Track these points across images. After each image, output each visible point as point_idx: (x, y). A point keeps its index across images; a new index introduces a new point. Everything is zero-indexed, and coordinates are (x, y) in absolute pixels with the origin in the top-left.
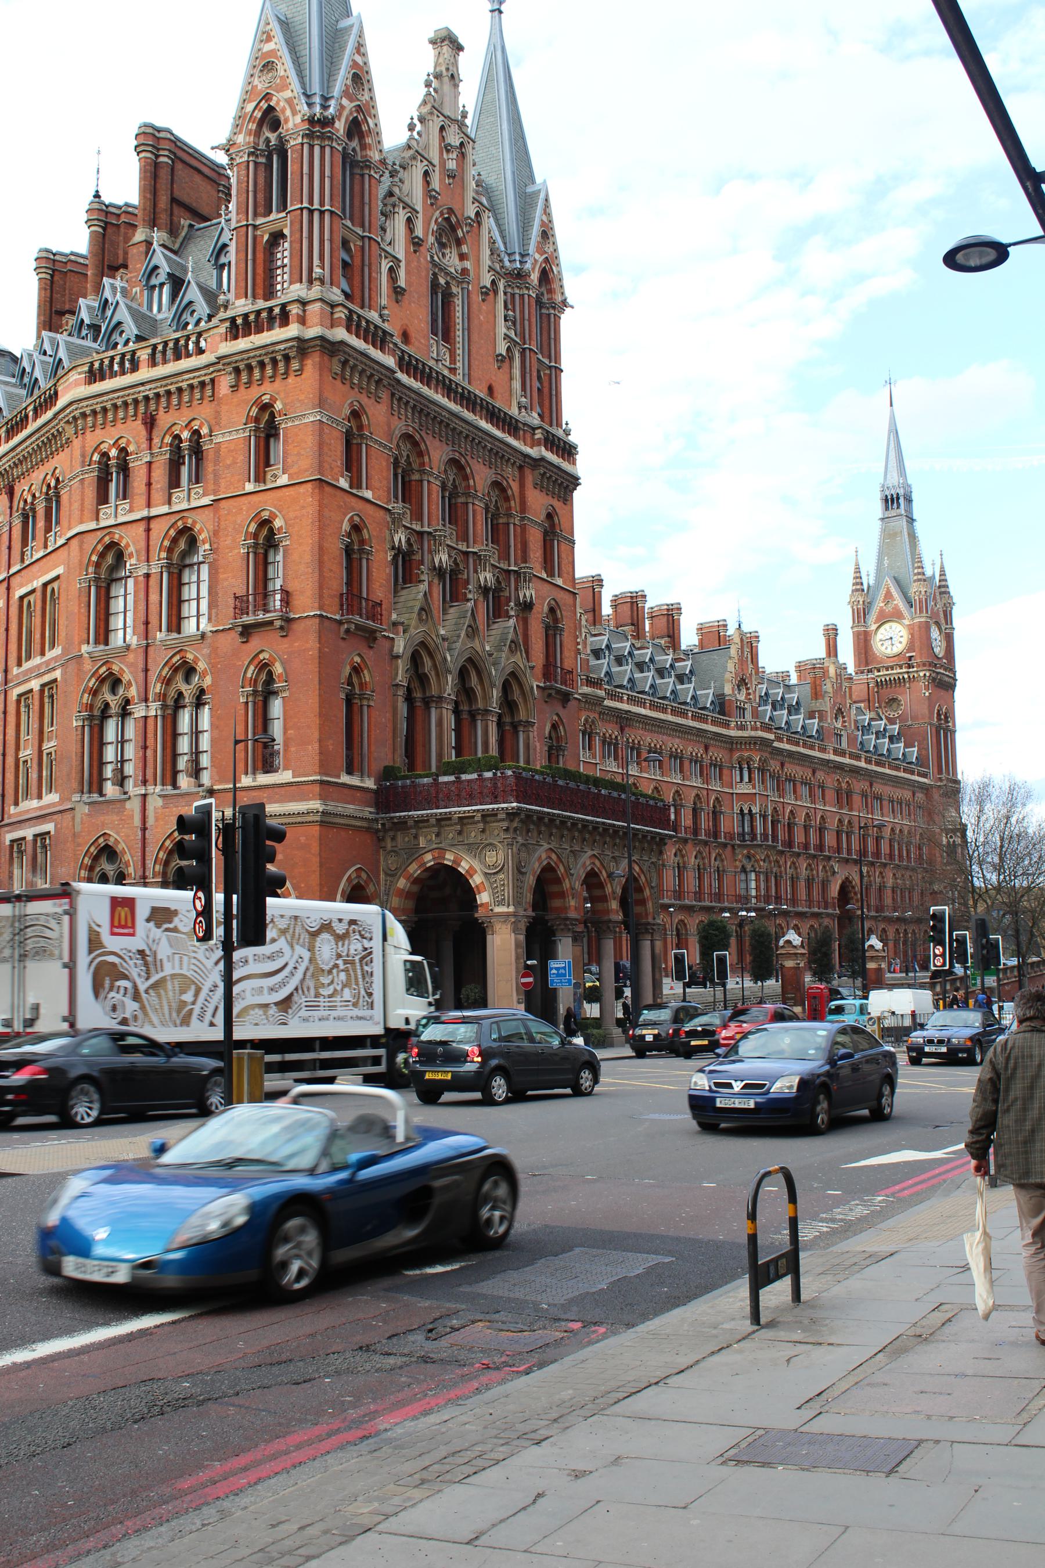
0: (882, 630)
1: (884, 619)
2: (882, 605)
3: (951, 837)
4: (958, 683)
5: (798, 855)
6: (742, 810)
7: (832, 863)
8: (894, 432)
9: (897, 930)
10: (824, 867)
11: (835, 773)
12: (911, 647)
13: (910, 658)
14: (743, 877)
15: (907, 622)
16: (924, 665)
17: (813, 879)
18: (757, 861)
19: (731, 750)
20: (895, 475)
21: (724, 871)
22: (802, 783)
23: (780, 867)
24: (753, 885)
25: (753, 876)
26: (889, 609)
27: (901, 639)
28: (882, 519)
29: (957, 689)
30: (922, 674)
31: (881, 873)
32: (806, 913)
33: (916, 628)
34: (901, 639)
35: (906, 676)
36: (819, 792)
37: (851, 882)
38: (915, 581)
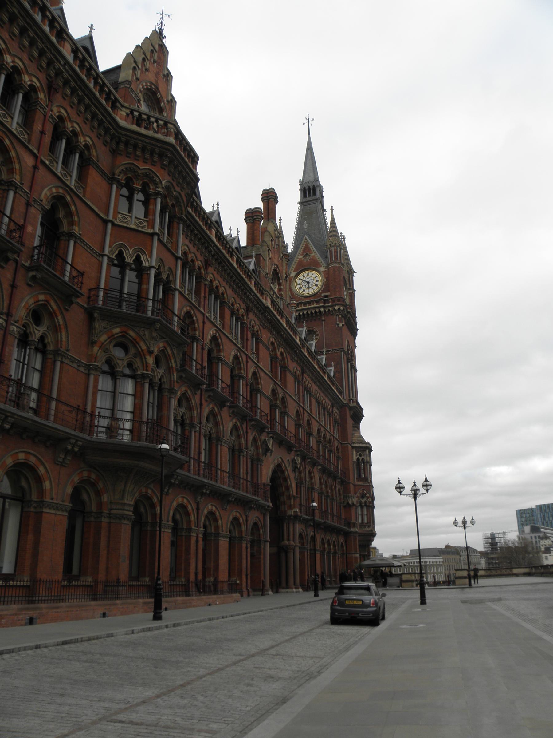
0: (301, 277)
1: (302, 269)
2: (301, 257)
3: (360, 455)
4: (358, 332)
5: (222, 404)
6: (120, 255)
7: (264, 437)
8: (310, 149)
9: (323, 539)
10: (255, 440)
11: (271, 333)
12: (326, 287)
13: (327, 296)
14: (105, 383)
15: (322, 269)
16: (339, 300)
17: (240, 451)
18: (140, 354)
19: (114, 152)
20: (312, 175)
21: (56, 352)
22: (232, 314)
23: (190, 409)
24: (128, 404)
25: (129, 386)
26: (307, 260)
27: (317, 283)
28: (299, 203)
29: (358, 337)
30: (336, 308)
31: (310, 473)
32: (229, 494)
33: (331, 272)
34: (317, 283)
35: (322, 310)
36: (251, 343)
37: (283, 472)
38: (331, 236)
